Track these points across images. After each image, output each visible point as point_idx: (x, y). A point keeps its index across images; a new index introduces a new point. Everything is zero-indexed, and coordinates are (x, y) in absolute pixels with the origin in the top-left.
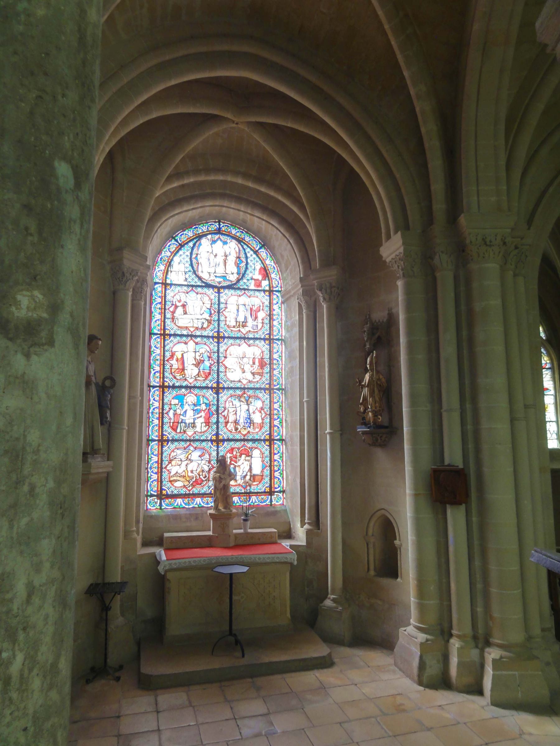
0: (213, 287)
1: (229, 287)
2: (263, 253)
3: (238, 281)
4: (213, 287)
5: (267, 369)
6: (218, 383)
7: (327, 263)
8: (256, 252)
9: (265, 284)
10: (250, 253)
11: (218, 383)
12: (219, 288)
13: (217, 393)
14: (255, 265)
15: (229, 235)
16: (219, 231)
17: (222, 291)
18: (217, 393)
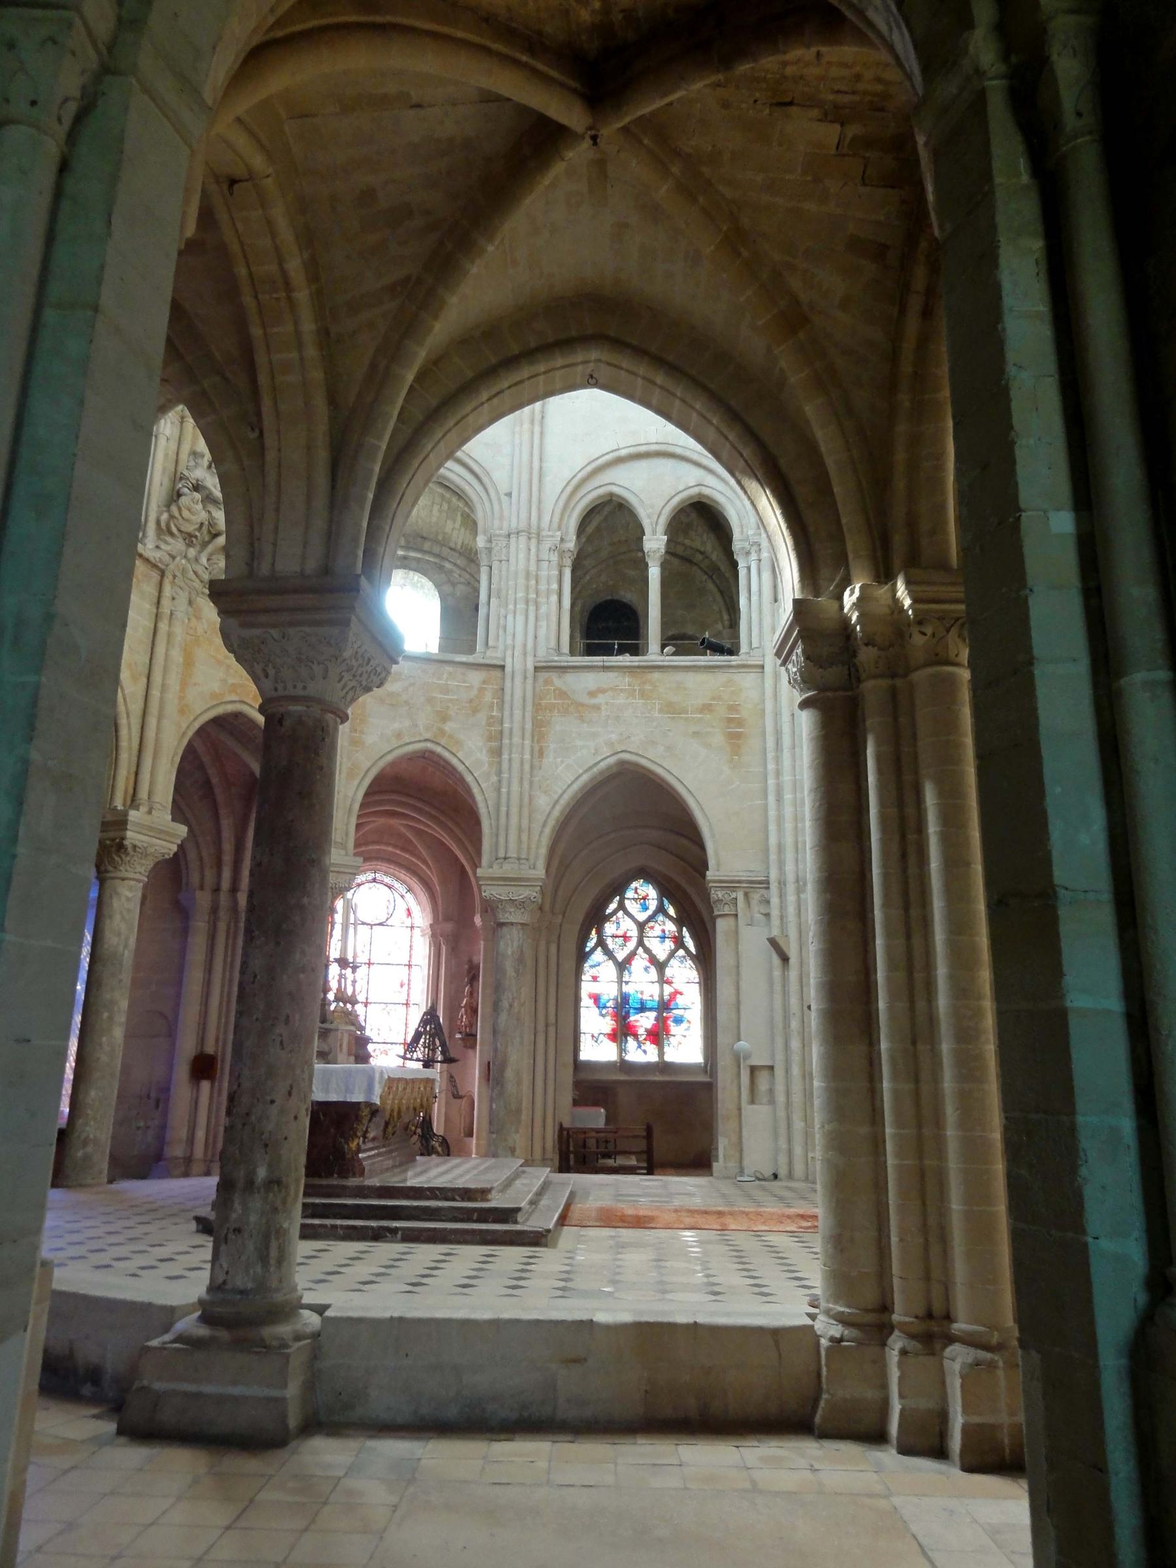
0: (368, 924)
1: (381, 924)
2: (409, 896)
3: (387, 919)
4: (368, 924)
5: (406, 987)
6: (367, 999)
7: (447, 918)
8: (402, 896)
9: (408, 922)
10: (397, 895)
11: (367, 999)
12: (372, 925)
13: (366, 1006)
14: (401, 906)
15: (382, 883)
16: (374, 880)
17: (374, 927)
18: (366, 1006)
